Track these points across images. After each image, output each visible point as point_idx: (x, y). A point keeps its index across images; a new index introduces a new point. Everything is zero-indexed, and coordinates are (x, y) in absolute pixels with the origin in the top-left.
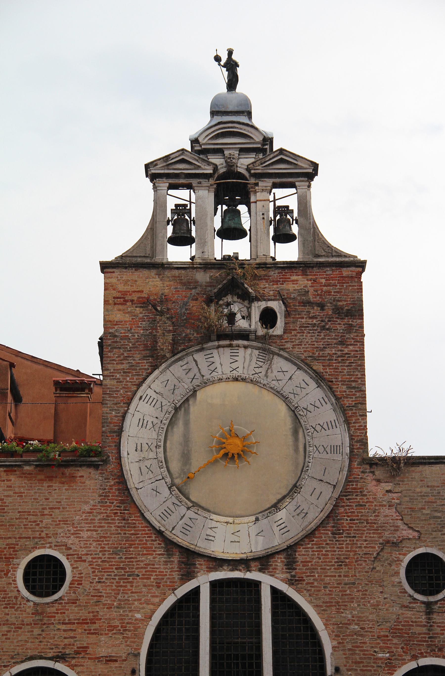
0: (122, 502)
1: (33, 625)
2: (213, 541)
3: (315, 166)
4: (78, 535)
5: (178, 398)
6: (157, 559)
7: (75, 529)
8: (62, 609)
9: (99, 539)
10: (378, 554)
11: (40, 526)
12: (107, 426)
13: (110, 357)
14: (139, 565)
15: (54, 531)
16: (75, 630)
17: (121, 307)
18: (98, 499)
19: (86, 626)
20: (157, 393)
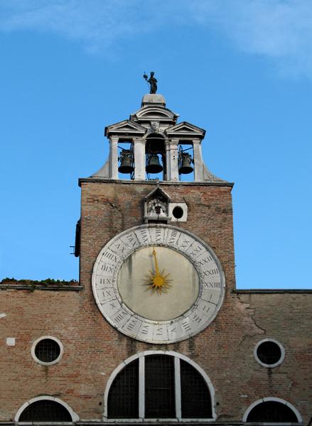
0: (93, 311)
3: (204, 132)
5: (126, 254)
10: (242, 342)
17: (91, 204)
18: (79, 309)
19: (72, 379)
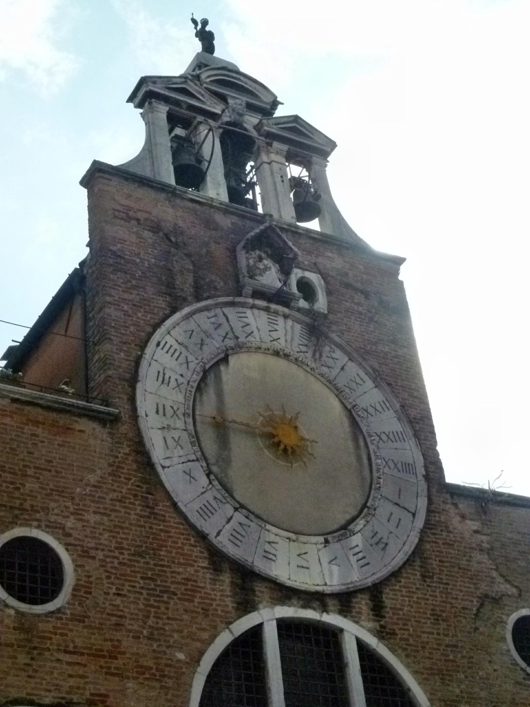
0: (144, 481)
1: (16, 647)
2: (274, 561)
4: (80, 517)
6: (200, 574)
7: (76, 507)
8: (62, 628)
9: (112, 528)
10: (478, 610)
11: (22, 491)
12: (115, 369)
13: (113, 280)
14: (175, 577)
15: (44, 503)
16: (85, 666)
19: (102, 662)
20: (179, 343)
